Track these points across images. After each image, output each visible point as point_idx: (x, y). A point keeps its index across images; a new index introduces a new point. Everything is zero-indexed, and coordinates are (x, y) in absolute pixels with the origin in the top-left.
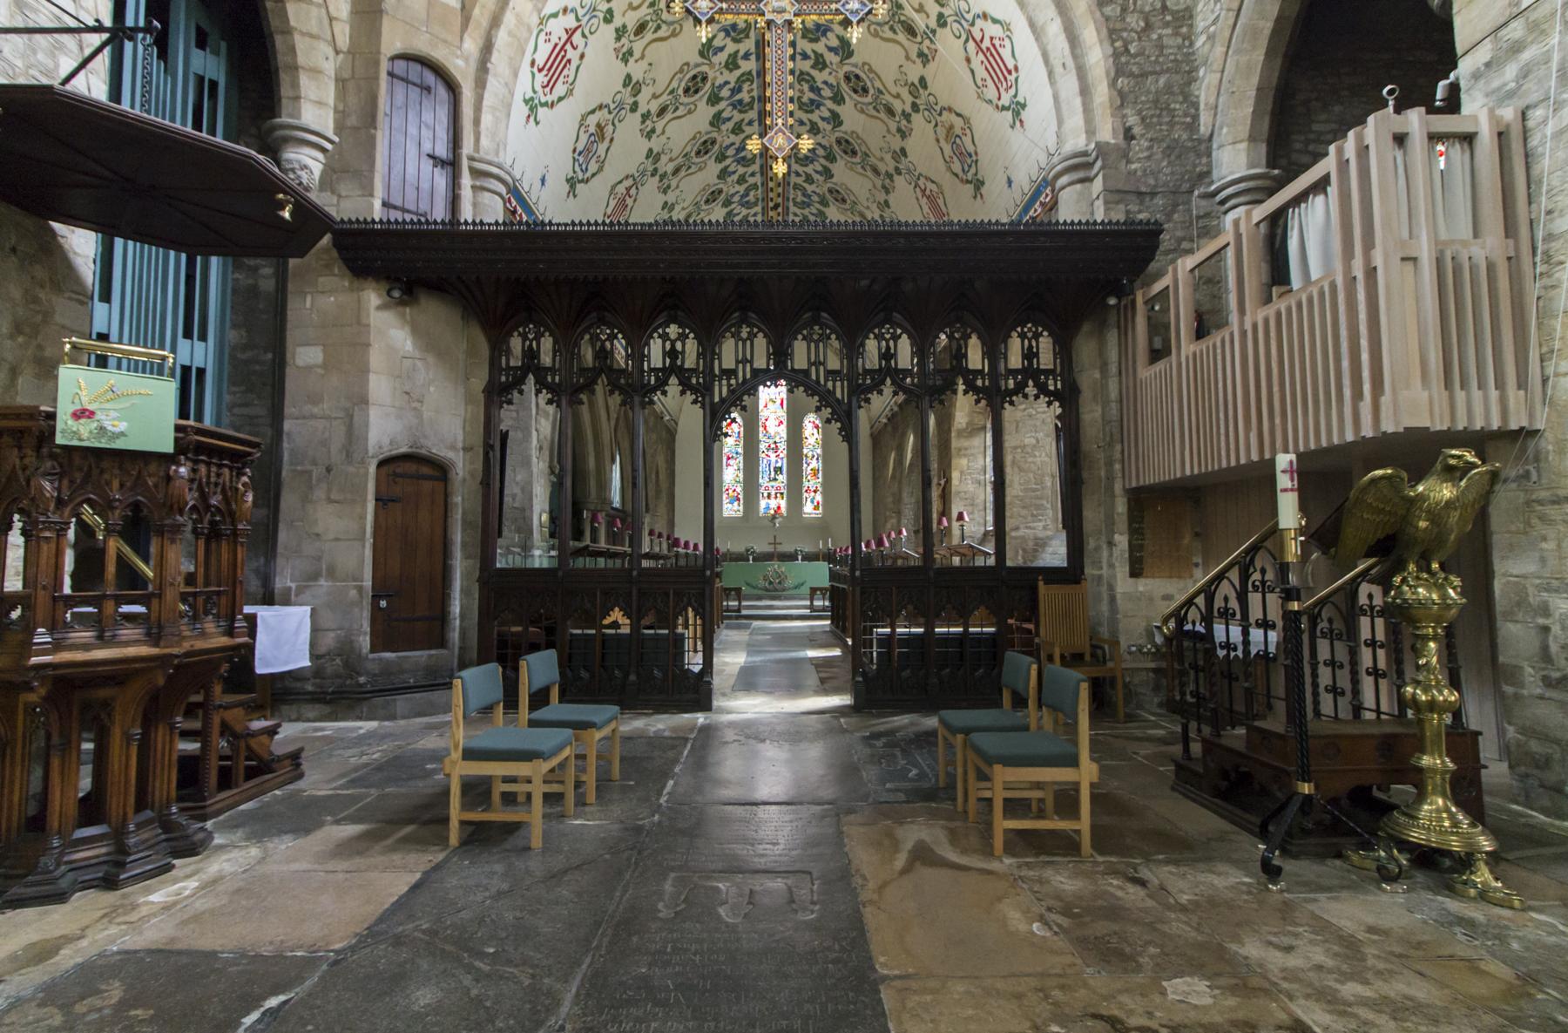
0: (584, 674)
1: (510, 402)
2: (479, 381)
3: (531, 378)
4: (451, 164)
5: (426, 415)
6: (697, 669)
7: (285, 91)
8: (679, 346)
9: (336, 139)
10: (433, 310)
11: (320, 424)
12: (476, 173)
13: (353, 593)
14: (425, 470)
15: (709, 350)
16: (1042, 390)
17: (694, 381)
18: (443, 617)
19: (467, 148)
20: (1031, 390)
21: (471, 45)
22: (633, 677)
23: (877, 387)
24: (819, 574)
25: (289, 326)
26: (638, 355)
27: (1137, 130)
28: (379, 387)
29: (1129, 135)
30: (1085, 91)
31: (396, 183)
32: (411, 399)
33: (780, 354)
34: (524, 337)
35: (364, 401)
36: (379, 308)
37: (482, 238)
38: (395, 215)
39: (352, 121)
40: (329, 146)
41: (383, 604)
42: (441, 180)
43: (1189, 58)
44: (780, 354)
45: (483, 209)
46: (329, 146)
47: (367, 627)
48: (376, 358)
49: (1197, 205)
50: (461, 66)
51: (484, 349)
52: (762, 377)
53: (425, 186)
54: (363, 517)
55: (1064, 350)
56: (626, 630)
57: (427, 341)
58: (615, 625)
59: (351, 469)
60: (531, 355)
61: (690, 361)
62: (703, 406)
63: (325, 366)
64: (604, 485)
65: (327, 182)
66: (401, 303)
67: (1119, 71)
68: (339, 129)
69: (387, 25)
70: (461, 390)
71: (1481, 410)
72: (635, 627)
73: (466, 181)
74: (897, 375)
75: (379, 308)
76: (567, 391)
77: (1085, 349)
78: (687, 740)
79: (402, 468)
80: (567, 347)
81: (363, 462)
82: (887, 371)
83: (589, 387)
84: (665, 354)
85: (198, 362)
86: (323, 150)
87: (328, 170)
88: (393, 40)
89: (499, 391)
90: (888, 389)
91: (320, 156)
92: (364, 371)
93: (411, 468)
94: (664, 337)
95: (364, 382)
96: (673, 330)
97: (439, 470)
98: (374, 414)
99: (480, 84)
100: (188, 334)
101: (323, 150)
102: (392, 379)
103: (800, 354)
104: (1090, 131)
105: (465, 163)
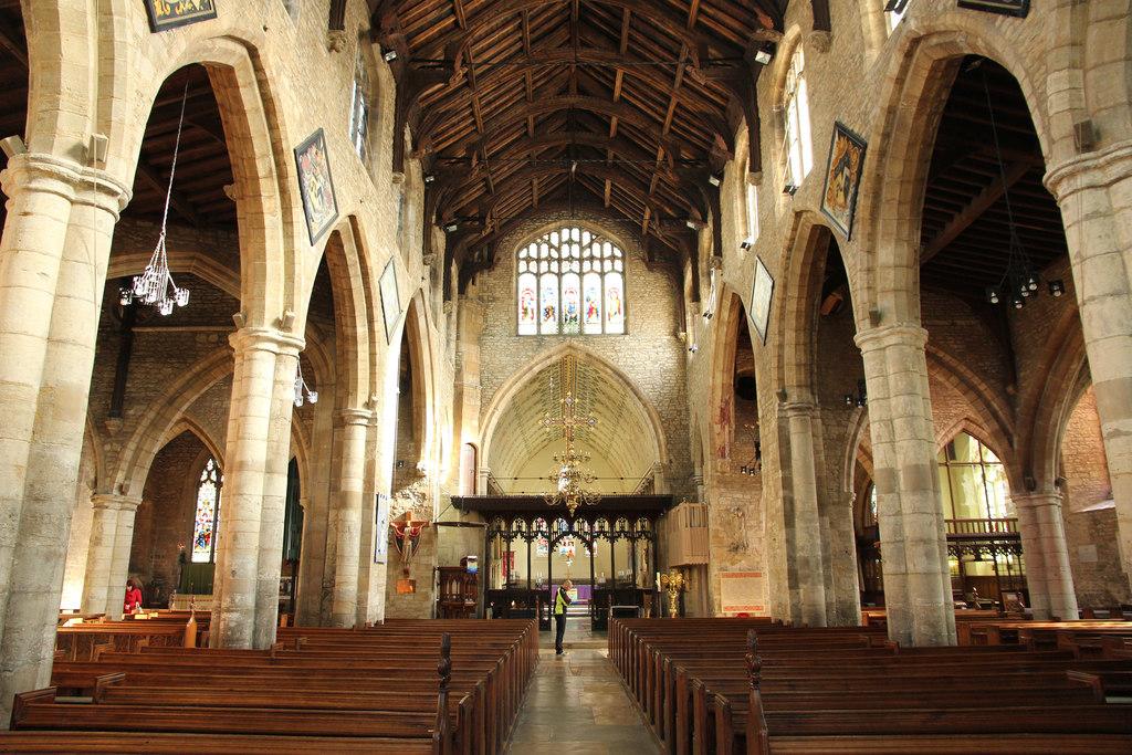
23: (598, 536)
26: (529, 526)
27: (674, 460)
29: (671, 462)
30: (660, 446)
33: (571, 527)
43: (688, 439)
44: (571, 527)
50: (479, 445)
52: (565, 534)
71: (698, 560)
74: (604, 533)
82: (602, 532)
90: (602, 536)
96: (539, 519)
99: (483, 445)
103: (576, 527)
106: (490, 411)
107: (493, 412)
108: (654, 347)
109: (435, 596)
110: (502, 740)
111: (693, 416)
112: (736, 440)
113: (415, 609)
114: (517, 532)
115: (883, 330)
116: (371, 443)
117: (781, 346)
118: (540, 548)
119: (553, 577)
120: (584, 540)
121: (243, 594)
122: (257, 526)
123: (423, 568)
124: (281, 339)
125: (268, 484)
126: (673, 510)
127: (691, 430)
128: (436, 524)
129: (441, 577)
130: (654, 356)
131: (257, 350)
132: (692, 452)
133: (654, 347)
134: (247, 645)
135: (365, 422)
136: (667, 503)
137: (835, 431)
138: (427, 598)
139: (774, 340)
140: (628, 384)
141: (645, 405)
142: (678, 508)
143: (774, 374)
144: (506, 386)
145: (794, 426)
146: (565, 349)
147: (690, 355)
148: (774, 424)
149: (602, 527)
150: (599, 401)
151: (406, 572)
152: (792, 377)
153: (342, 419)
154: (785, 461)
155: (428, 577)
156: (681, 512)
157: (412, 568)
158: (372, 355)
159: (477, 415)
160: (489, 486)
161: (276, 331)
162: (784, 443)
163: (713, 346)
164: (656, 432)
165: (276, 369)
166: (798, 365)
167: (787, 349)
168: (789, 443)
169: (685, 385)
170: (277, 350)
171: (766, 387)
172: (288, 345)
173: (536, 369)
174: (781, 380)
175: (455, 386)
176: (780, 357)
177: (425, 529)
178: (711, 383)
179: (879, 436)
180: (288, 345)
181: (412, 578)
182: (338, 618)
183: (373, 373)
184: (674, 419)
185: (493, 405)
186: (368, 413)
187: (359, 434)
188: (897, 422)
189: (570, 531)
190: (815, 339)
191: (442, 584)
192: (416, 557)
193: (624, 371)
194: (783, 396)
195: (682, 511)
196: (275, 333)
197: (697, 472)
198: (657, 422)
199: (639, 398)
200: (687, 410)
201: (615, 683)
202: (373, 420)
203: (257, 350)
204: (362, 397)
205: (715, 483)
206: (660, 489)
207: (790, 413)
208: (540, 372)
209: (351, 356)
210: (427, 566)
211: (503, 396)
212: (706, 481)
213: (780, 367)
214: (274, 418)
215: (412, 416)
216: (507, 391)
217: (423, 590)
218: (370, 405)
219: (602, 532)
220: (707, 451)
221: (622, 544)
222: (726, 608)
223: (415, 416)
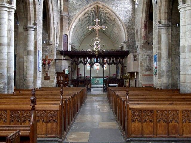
16: (120, 64)
19: (68, 41)
20: (120, 64)
21: (69, 32)
24: (101, 80)
26: (84, 60)
29: (129, 40)
30: (125, 35)
35: (62, 65)
39: (60, 41)
44: (97, 60)
49: (135, 47)
50: (68, 34)
52: (96, 62)
55: (122, 60)
67: (128, 34)
69: (63, 32)
73: (68, 44)
77: (124, 59)
88: (63, 33)
99: (69, 35)
104: (126, 39)
106: (72, 24)
107: (73, 24)
108: (125, 3)
109: (55, 81)
110: (73, 117)
111: (136, 26)
112: (148, 34)
113: (50, 85)
114: (80, 62)
115: (185, 5)
116: (36, 36)
117: (160, 7)
118: (88, 67)
119: (91, 76)
120: (101, 64)
121: (4, 79)
122: (6, 61)
123: (52, 73)
124: (9, 7)
125: (9, 49)
126: (129, 55)
127: (135, 30)
128: (55, 59)
129: (57, 75)
130: (124, 6)
131: (2, 10)
132: (136, 37)
133: (125, 3)
134: (6, 93)
135: (33, 29)
136: (126, 53)
137: (175, 33)
138: (53, 81)
139: (158, 5)
140: (116, 15)
141: (121, 22)
142: (130, 55)
143: (158, 15)
144: (76, 15)
145: (163, 32)
146: (96, 3)
147: (136, 6)
148: (157, 30)
149: (81, 60)
150: (107, 20)
151: (47, 74)
152: (163, 16)
153: (27, 28)
154: (159, 42)
156: (131, 56)
157: (48, 73)
158: (35, 8)
159: (67, 25)
160: (72, 47)
161: (7, 4)
162: (160, 36)
163: (142, 4)
164: (124, 30)
165: (9, 16)
166: (165, 13)
167: (162, 7)
168: (161, 36)
169: (134, 15)
170: (8, 10)
171: (156, 19)
172: (11, 8)
173: (86, 10)
174: (160, 17)
175: (60, 16)
176: (160, 10)
178: (141, 16)
179: (182, 37)
180: (11, 8)
181: (48, 76)
182: (28, 87)
183: (35, 14)
184: (131, 27)
185: (72, 22)
186: (34, 27)
187: (32, 33)
188: (187, 33)
189: (97, 61)
190: (171, 4)
191: (57, 78)
193: (115, 11)
194: (160, 22)
195: (131, 56)
196: (7, 5)
197: (137, 43)
198: (125, 28)
199: (120, 20)
200: (135, 24)
201: (107, 104)
202: (36, 29)
203: (2, 10)
204: (32, 22)
205: (141, 47)
206: (125, 49)
207: (162, 27)
208: (88, 11)
209: (28, 9)
210: (53, 72)
211: (76, 19)
212: (139, 47)
213: (160, 13)
214: (9, 30)
215: (47, 26)
216: (77, 17)
217: (52, 80)
218: (35, 24)
219: (107, 62)
220: (139, 37)
221: (113, 66)
222: (143, 85)
223: (48, 26)
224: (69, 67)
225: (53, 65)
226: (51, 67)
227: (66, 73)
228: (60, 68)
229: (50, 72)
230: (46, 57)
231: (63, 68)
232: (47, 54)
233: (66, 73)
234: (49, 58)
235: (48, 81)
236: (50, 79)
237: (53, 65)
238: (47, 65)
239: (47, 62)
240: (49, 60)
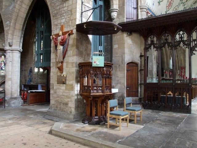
0: (163, 104)
1: (148, 51)
2: (143, 47)
3: (152, 46)
4: (137, 8)
5: (134, 54)
6: (187, 105)
7: (111, 4)
8: (183, 36)
9: (119, 9)
10: (135, 35)
11: (118, 58)
12: (141, 9)
13: (123, 87)
14: (134, 65)
15: (189, 35)
17: (186, 43)
18: (138, 91)
19: (139, 5)
22: (173, 105)
25: (113, 42)
28: (127, 51)
31: (128, 14)
32: (131, 52)
34: (151, 38)
35: (124, 53)
36: (126, 37)
37: (143, 21)
38: (128, 20)
40: (118, 11)
41: (128, 89)
42: (135, 11)
45: (143, 16)
46: (118, 11)
47: (126, 93)
48: (126, 46)
51: (144, 42)
53: (133, 13)
54: (125, 74)
56: (172, 96)
57: (134, 41)
58: (170, 95)
59: (122, 65)
60: (152, 41)
61: (185, 39)
62: (188, 48)
63: (118, 48)
64: (168, 64)
65: (118, 17)
66: (130, 35)
68: (119, 8)
70: (140, 49)
72: (174, 95)
73: (139, 10)
75: (126, 37)
76: (159, 48)
78: (184, 118)
79: (130, 65)
80: (159, 39)
81: (124, 64)
83: (164, 46)
84: (179, 38)
85: (101, 50)
86: (117, 12)
87: (118, 15)
89: (146, 49)
91: (116, 13)
92: (124, 48)
93: (132, 64)
94: (179, 34)
95: (124, 50)
96: (181, 33)
97: (136, 64)
98: (126, 55)
100: (100, 45)
101: (117, 12)
102: (129, 48)
105: (139, 7)
113: (67, 96)
123: (70, 66)
138: (72, 88)
155: (73, 72)
177: (73, 37)
192: (65, 59)
210: (73, 63)
217: (70, 83)
224: (141, 56)
225: (73, 46)
226: (70, 52)
227: (94, 65)
228: (121, 60)
229: (67, 62)
230: (62, 29)
231: (126, 60)
232: (63, 21)
233: (94, 65)
234: (65, 30)
235: (63, 87)
236: (67, 82)
237: (73, 46)
238: (60, 48)
239: (60, 39)
240: (64, 34)
